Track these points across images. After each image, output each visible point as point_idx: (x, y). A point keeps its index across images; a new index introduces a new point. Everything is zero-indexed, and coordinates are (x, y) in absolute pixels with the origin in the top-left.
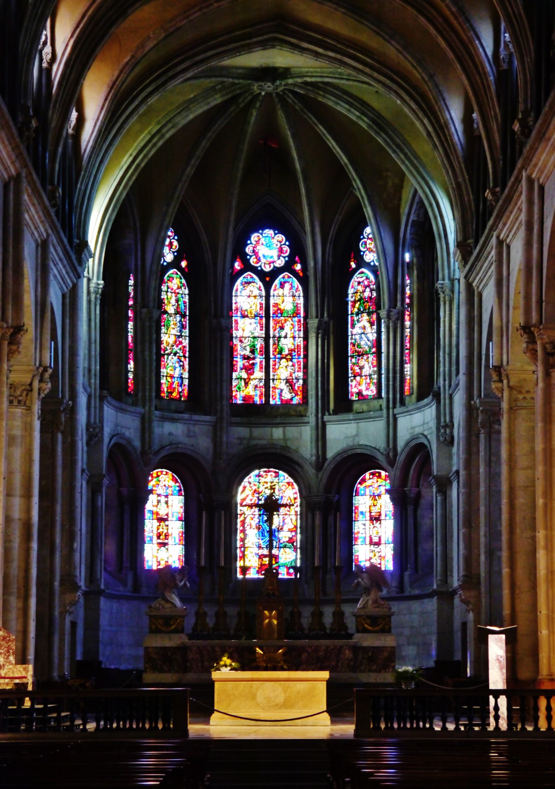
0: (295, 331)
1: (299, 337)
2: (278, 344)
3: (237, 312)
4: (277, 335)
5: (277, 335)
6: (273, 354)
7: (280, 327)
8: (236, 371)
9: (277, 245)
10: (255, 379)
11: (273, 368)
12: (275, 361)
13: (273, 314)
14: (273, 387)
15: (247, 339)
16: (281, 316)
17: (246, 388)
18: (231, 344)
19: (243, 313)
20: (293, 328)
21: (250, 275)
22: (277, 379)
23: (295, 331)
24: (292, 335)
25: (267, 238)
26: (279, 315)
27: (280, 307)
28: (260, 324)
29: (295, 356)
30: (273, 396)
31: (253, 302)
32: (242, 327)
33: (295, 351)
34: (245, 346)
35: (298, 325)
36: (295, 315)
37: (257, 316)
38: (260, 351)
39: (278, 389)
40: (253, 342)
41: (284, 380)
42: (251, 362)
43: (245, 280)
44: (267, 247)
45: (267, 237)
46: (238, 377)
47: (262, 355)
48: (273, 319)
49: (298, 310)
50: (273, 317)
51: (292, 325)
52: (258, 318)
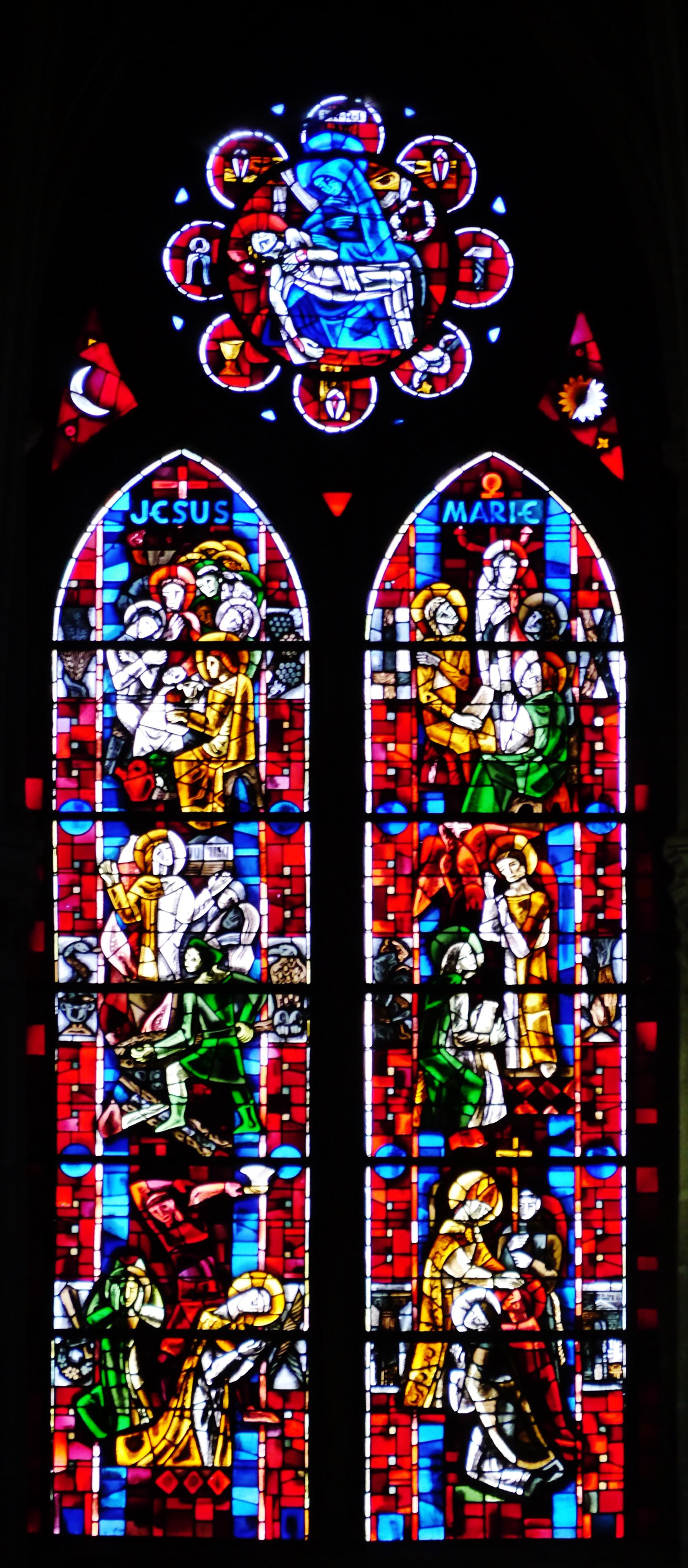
0: (560, 936)
1: (596, 990)
2: (428, 1049)
3: (85, 785)
4: (421, 969)
5: (421, 969)
6: (384, 1129)
7: (439, 900)
8: (75, 1271)
9: (413, 221)
10: (236, 1338)
11: (381, 1247)
12: (401, 1182)
13: (383, 796)
14: (381, 1404)
15: (169, 1000)
16: (453, 813)
17: (160, 1411)
18: (36, 1044)
19: (136, 784)
20: (551, 909)
21: (196, 473)
22: (414, 1338)
23: (560, 936)
24: (539, 969)
25: (333, 167)
26: (436, 806)
27: (438, 732)
28: (275, 878)
29: (565, 1140)
30: (382, 1475)
31: (218, 696)
32: (125, 899)
33: (564, 1106)
34: (155, 1064)
35: (589, 877)
36: (562, 799)
37: (253, 816)
38: (277, 1103)
39: (426, 1416)
40: (220, 1029)
41: (470, 1340)
42: (202, 1192)
43: (151, 511)
44: (336, 238)
45: (336, 152)
46: (97, 1316)
47: (292, 1135)
48: (383, 838)
49: (594, 759)
50: (380, 821)
51: (535, 880)
52: (258, 828)
